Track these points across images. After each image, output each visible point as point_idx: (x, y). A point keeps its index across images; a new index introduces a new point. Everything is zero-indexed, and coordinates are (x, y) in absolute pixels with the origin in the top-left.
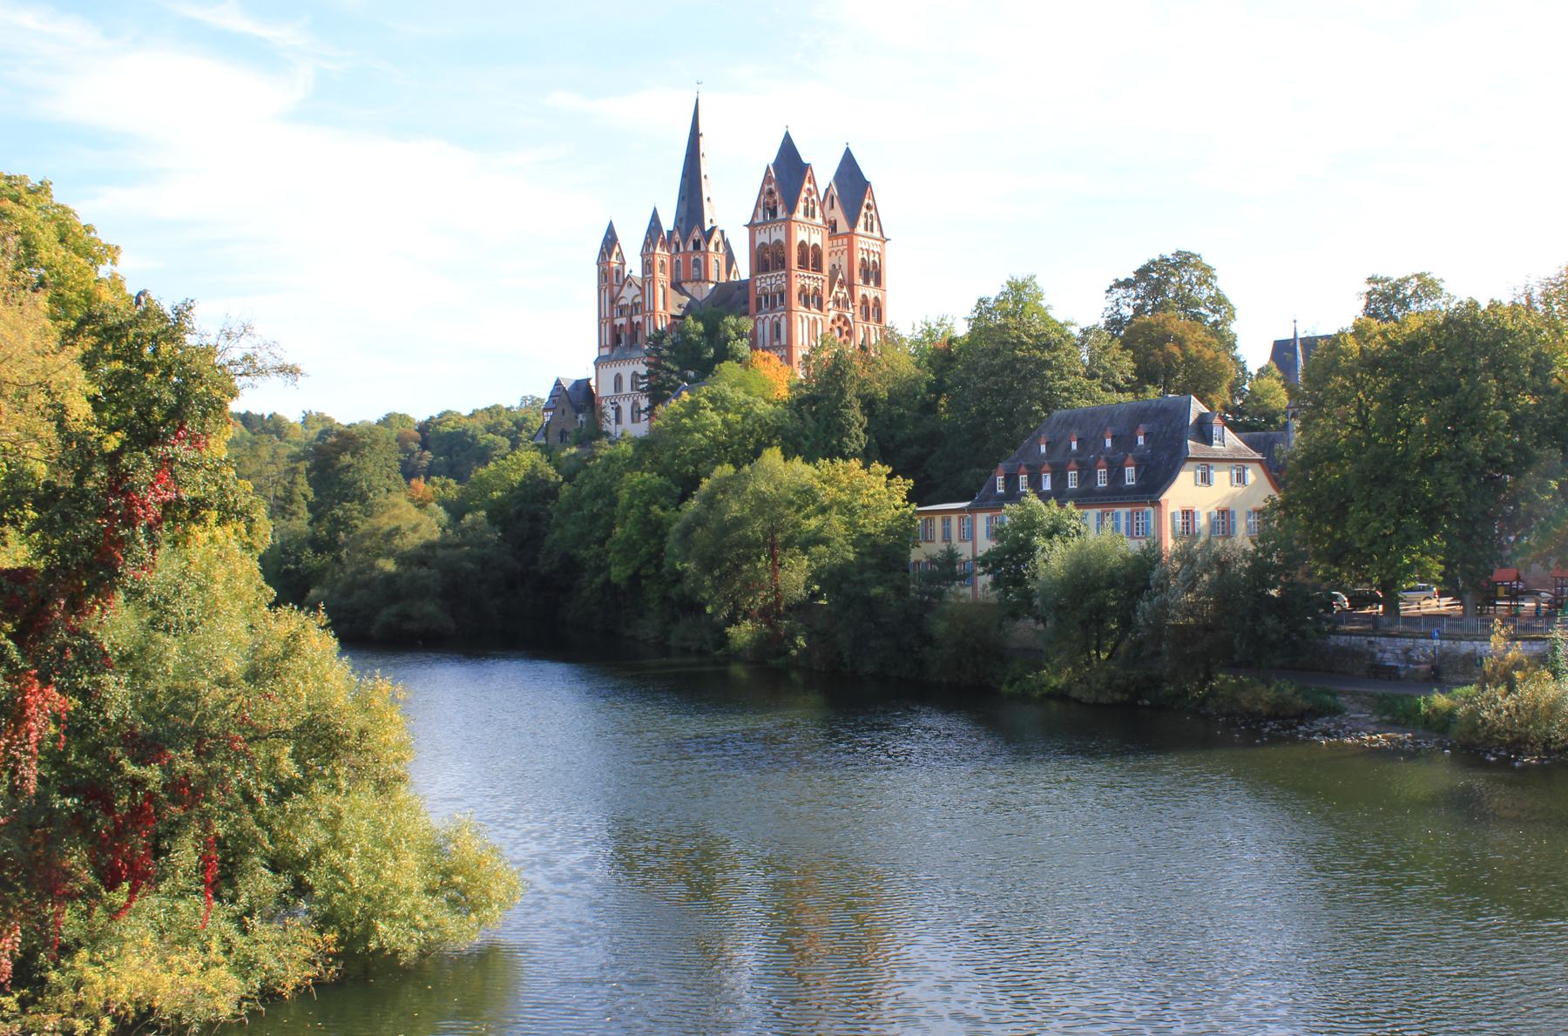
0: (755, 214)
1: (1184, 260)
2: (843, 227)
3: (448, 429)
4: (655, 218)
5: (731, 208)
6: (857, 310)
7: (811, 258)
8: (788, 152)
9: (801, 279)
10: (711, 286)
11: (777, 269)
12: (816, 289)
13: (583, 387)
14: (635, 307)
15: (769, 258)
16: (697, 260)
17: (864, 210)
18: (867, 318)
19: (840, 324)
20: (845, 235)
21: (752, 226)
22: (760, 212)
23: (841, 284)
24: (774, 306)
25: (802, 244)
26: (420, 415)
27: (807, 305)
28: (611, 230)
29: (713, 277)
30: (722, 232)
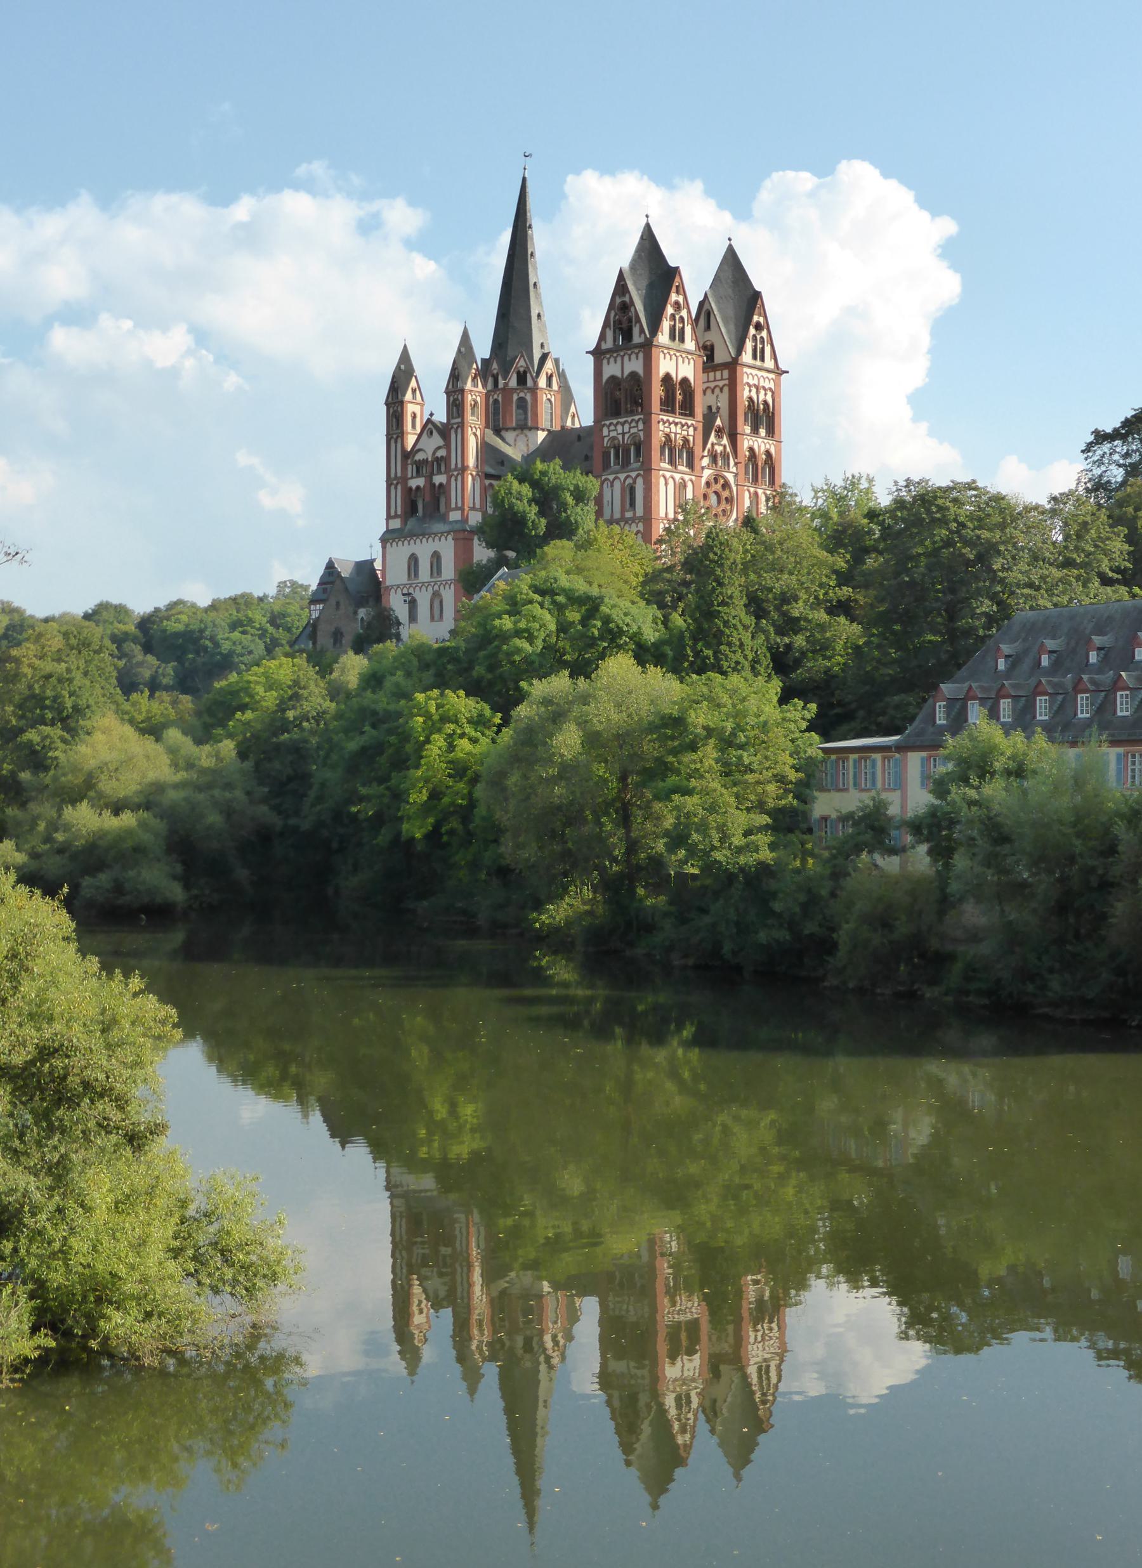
0: (602, 337)
2: (720, 357)
3: (180, 627)
4: (465, 338)
5: (570, 328)
6: (742, 466)
7: (679, 398)
8: (649, 246)
10: (541, 436)
11: (632, 413)
12: (686, 440)
13: (365, 568)
14: (438, 460)
15: (621, 397)
16: (522, 403)
17: (752, 331)
18: (755, 480)
19: (718, 487)
20: (725, 366)
21: (598, 354)
22: (610, 334)
23: (719, 435)
24: (626, 464)
25: (667, 378)
26: (142, 604)
27: (672, 462)
28: (405, 357)
29: (544, 420)
30: (557, 361)
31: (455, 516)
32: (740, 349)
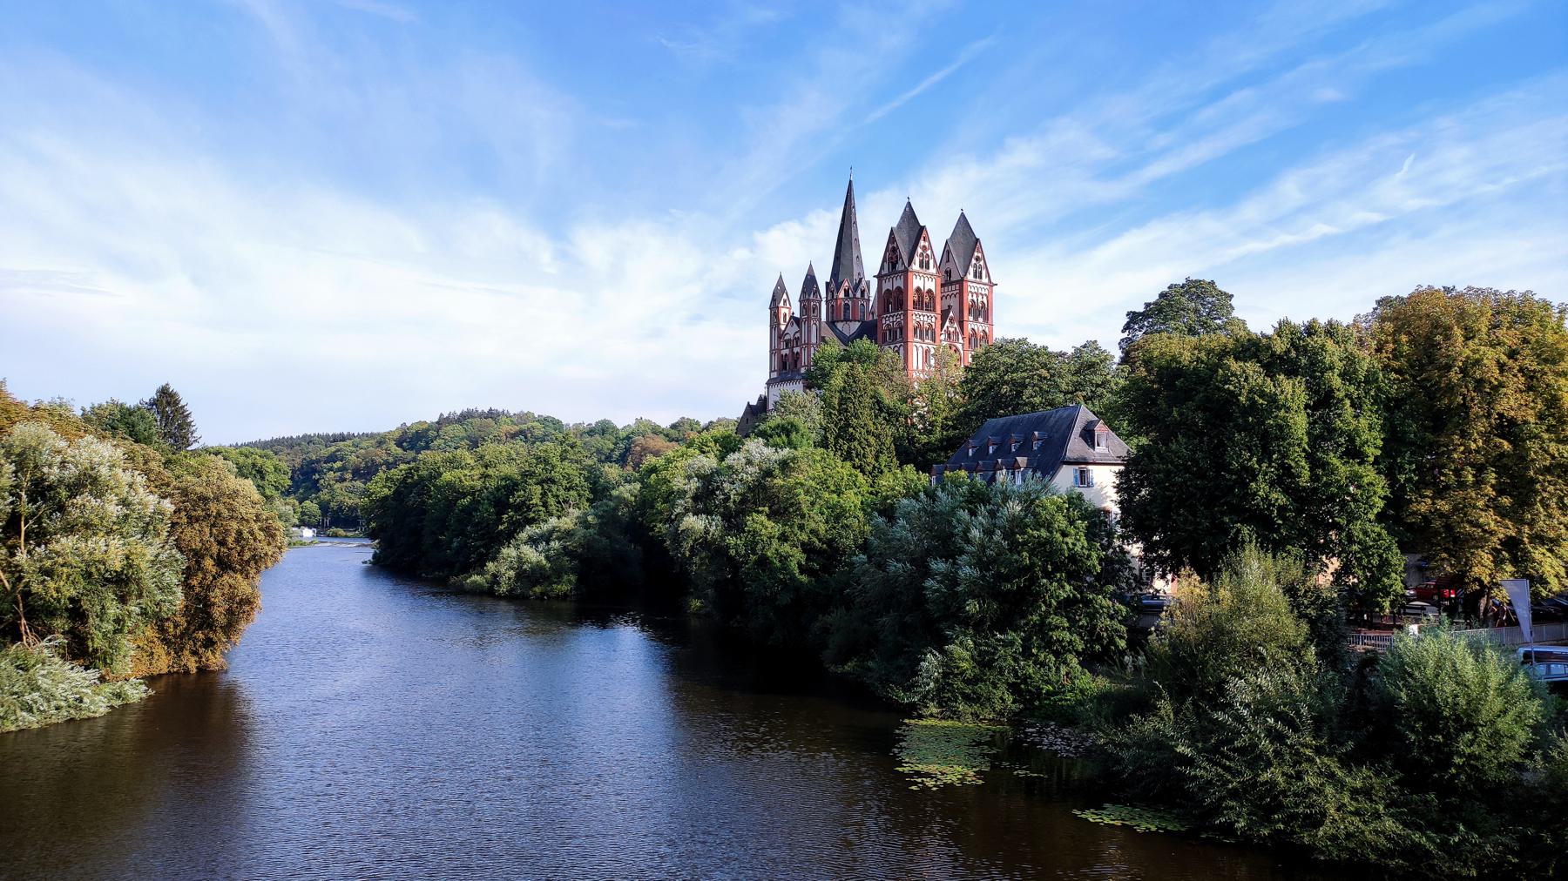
0: (882, 267)
1: (1196, 290)
7: (925, 301)
8: (910, 215)
9: (916, 317)
14: (797, 339)
21: (880, 277)
25: (918, 290)
28: (780, 283)
30: (868, 283)
31: (803, 370)
32: (966, 272)
